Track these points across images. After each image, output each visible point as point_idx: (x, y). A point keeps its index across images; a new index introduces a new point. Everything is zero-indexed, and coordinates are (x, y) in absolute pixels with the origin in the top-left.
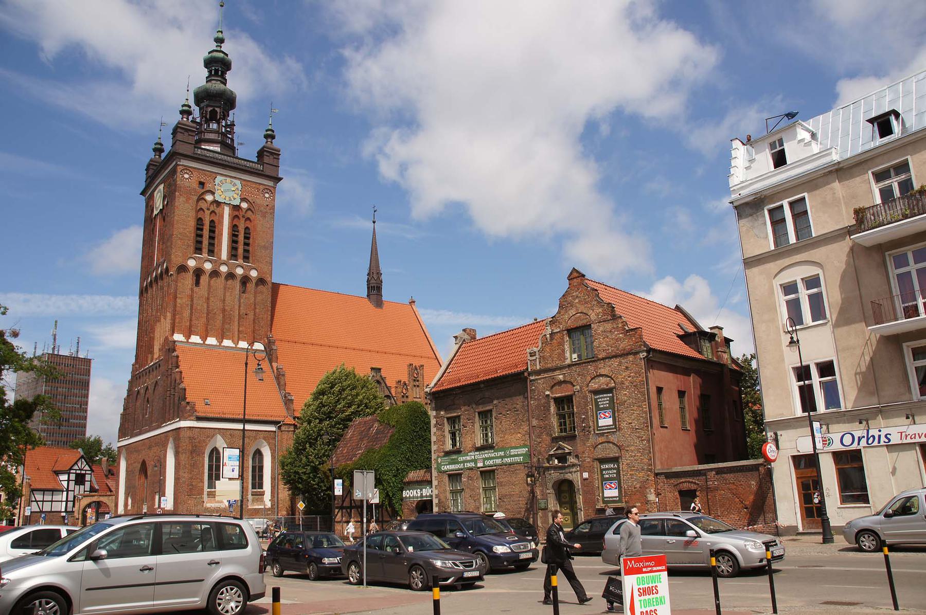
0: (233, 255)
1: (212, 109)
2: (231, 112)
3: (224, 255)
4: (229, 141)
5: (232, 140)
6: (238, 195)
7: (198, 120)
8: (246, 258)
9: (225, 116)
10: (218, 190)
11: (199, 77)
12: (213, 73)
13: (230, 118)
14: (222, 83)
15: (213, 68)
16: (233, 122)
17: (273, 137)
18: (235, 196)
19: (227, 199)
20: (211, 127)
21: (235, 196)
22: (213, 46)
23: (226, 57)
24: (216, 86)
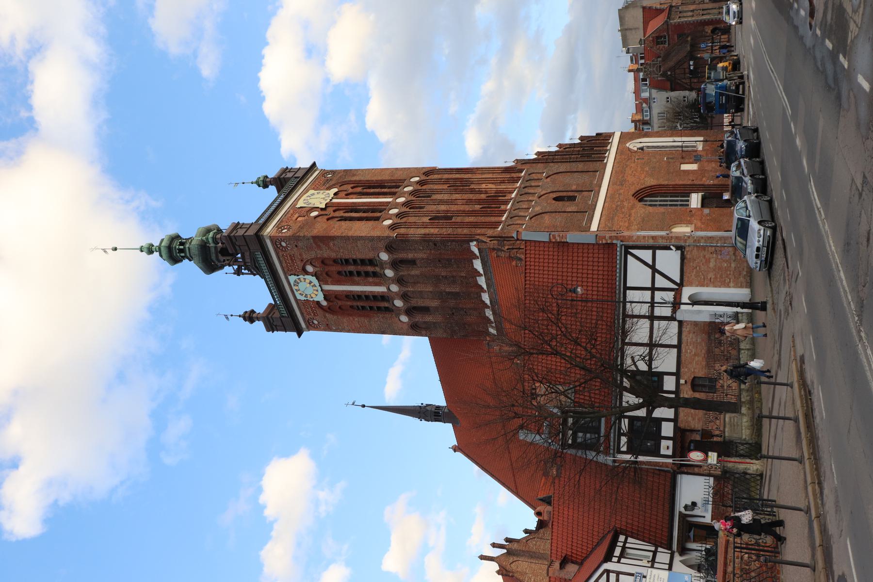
0: (393, 194)
3: (390, 200)
8: (398, 188)
12: (183, 255)
15: (177, 247)
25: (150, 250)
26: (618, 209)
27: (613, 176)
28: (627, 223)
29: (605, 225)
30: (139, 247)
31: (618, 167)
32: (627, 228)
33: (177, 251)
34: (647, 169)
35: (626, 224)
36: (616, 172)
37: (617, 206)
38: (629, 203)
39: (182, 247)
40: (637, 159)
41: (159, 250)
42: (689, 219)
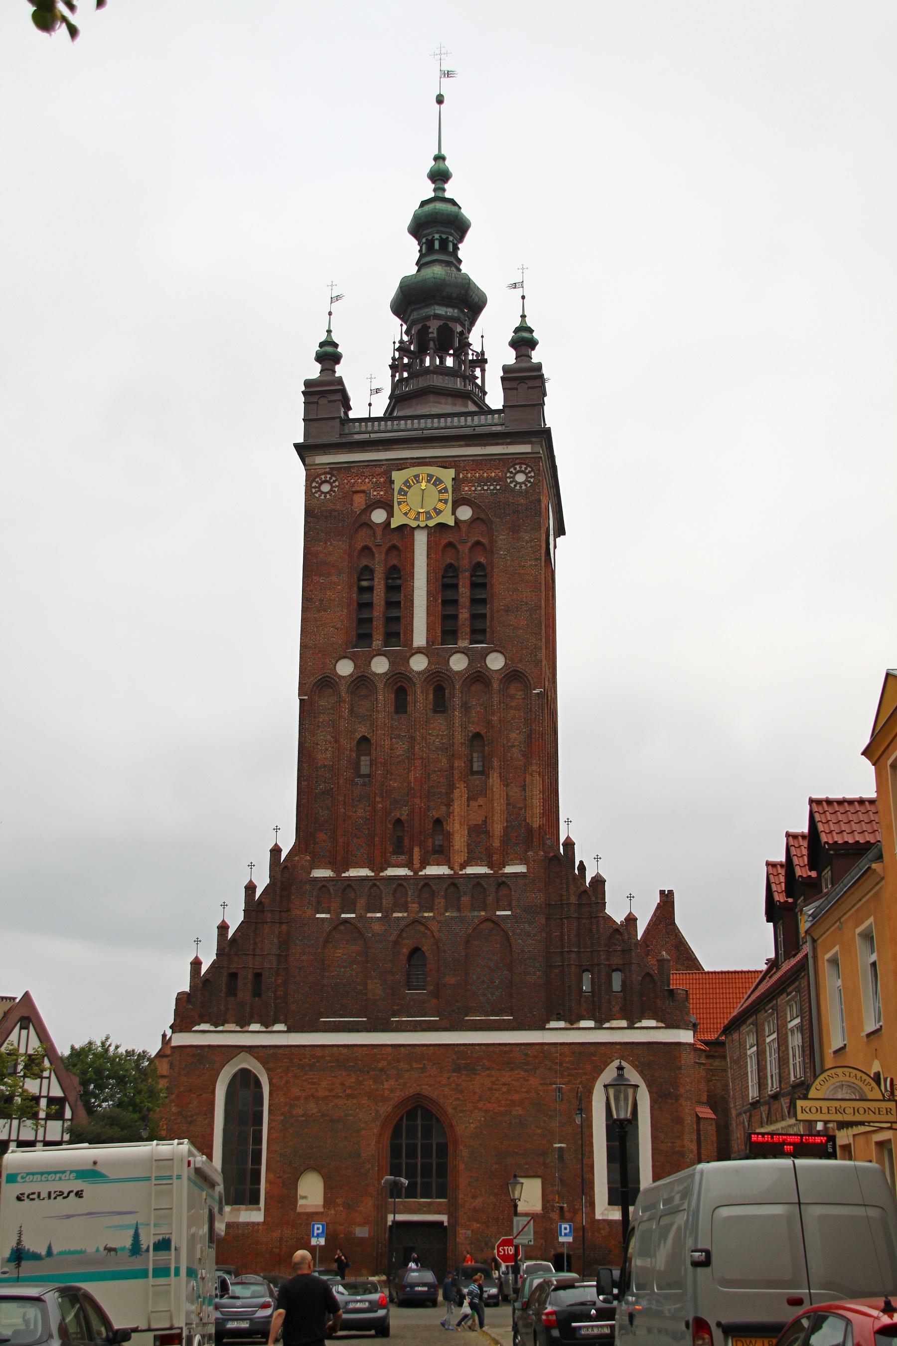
6: (446, 501)
10: (399, 503)
14: (448, 264)
17: (533, 344)
18: (440, 506)
21: (440, 506)
22: (429, 193)
25: (440, 176)
26: (371, 1073)
27: (491, 1049)
28: (327, 1093)
29: (323, 1057)
30: (443, 152)
31: (526, 1055)
32: (313, 1096)
33: (430, 238)
34: (518, 1111)
35: (321, 1093)
36: (505, 1052)
37: (382, 1070)
38: (392, 1090)
39: (437, 245)
40: (560, 1089)
41: (439, 198)
42: (340, 1201)
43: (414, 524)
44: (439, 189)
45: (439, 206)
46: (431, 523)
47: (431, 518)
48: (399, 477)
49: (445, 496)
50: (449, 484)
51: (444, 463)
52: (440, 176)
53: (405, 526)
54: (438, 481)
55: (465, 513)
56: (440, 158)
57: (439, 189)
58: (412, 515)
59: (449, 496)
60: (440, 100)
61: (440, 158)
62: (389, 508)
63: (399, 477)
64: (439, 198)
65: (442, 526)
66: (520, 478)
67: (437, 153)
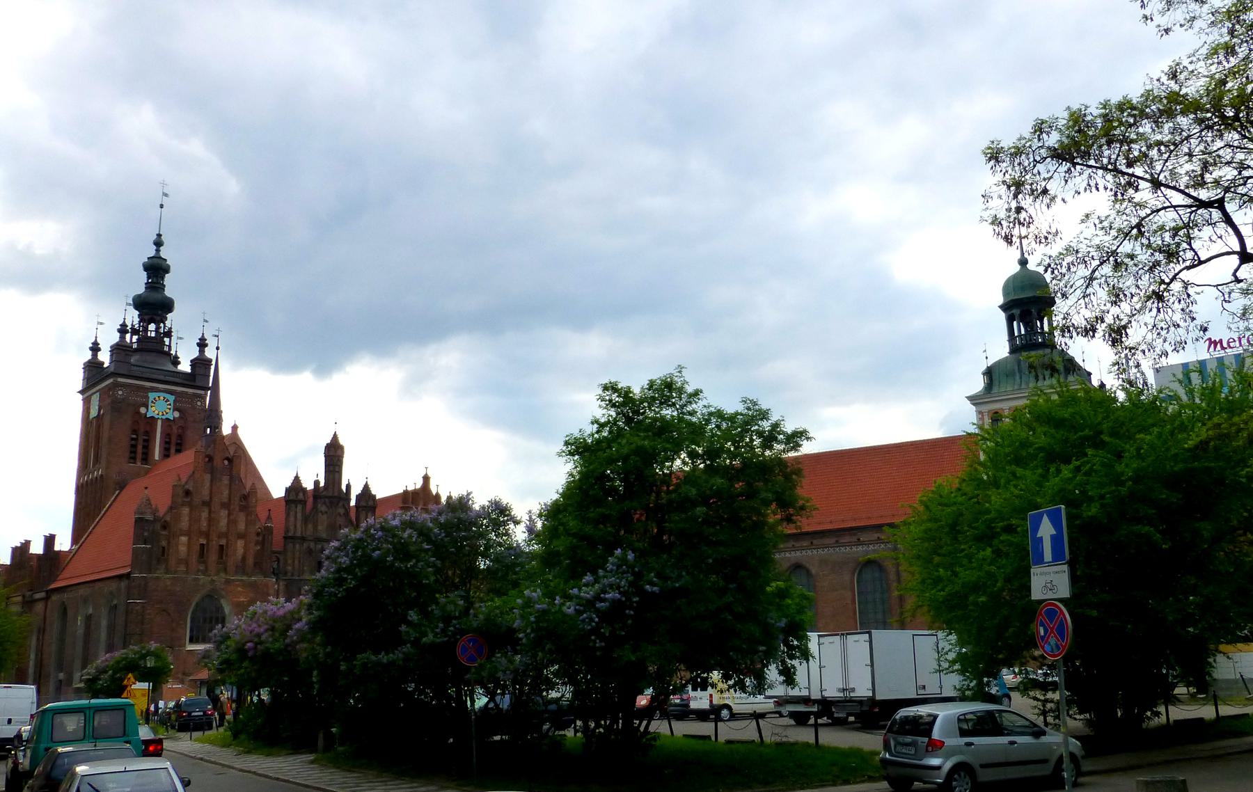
1: (150, 316)
2: (169, 316)
4: (166, 349)
5: (170, 346)
6: (170, 409)
7: (136, 326)
9: (163, 320)
11: (139, 282)
13: (168, 323)
16: (171, 328)
18: (168, 411)
19: (161, 413)
20: (149, 335)
21: (168, 411)
22: (152, 253)
23: (164, 262)
24: (155, 296)
25: (158, 243)
41: (157, 257)
43: (157, 417)
44: (158, 251)
45: (160, 261)
46: (164, 417)
47: (163, 415)
48: (152, 396)
49: (169, 407)
50: (172, 402)
51: (171, 393)
52: (158, 243)
53: (153, 417)
54: (167, 401)
55: (177, 414)
56: (159, 235)
57: (158, 251)
58: (157, 412)
59: (172, 407)
60: (162, 206)
61: (159, 235)
62: (147, 407)
63: (152, 396)
64: (157, 257)
65: (167, 419)
66: (199, 403)
67: (158, 233)
